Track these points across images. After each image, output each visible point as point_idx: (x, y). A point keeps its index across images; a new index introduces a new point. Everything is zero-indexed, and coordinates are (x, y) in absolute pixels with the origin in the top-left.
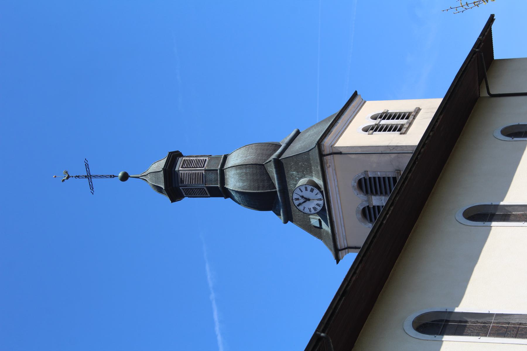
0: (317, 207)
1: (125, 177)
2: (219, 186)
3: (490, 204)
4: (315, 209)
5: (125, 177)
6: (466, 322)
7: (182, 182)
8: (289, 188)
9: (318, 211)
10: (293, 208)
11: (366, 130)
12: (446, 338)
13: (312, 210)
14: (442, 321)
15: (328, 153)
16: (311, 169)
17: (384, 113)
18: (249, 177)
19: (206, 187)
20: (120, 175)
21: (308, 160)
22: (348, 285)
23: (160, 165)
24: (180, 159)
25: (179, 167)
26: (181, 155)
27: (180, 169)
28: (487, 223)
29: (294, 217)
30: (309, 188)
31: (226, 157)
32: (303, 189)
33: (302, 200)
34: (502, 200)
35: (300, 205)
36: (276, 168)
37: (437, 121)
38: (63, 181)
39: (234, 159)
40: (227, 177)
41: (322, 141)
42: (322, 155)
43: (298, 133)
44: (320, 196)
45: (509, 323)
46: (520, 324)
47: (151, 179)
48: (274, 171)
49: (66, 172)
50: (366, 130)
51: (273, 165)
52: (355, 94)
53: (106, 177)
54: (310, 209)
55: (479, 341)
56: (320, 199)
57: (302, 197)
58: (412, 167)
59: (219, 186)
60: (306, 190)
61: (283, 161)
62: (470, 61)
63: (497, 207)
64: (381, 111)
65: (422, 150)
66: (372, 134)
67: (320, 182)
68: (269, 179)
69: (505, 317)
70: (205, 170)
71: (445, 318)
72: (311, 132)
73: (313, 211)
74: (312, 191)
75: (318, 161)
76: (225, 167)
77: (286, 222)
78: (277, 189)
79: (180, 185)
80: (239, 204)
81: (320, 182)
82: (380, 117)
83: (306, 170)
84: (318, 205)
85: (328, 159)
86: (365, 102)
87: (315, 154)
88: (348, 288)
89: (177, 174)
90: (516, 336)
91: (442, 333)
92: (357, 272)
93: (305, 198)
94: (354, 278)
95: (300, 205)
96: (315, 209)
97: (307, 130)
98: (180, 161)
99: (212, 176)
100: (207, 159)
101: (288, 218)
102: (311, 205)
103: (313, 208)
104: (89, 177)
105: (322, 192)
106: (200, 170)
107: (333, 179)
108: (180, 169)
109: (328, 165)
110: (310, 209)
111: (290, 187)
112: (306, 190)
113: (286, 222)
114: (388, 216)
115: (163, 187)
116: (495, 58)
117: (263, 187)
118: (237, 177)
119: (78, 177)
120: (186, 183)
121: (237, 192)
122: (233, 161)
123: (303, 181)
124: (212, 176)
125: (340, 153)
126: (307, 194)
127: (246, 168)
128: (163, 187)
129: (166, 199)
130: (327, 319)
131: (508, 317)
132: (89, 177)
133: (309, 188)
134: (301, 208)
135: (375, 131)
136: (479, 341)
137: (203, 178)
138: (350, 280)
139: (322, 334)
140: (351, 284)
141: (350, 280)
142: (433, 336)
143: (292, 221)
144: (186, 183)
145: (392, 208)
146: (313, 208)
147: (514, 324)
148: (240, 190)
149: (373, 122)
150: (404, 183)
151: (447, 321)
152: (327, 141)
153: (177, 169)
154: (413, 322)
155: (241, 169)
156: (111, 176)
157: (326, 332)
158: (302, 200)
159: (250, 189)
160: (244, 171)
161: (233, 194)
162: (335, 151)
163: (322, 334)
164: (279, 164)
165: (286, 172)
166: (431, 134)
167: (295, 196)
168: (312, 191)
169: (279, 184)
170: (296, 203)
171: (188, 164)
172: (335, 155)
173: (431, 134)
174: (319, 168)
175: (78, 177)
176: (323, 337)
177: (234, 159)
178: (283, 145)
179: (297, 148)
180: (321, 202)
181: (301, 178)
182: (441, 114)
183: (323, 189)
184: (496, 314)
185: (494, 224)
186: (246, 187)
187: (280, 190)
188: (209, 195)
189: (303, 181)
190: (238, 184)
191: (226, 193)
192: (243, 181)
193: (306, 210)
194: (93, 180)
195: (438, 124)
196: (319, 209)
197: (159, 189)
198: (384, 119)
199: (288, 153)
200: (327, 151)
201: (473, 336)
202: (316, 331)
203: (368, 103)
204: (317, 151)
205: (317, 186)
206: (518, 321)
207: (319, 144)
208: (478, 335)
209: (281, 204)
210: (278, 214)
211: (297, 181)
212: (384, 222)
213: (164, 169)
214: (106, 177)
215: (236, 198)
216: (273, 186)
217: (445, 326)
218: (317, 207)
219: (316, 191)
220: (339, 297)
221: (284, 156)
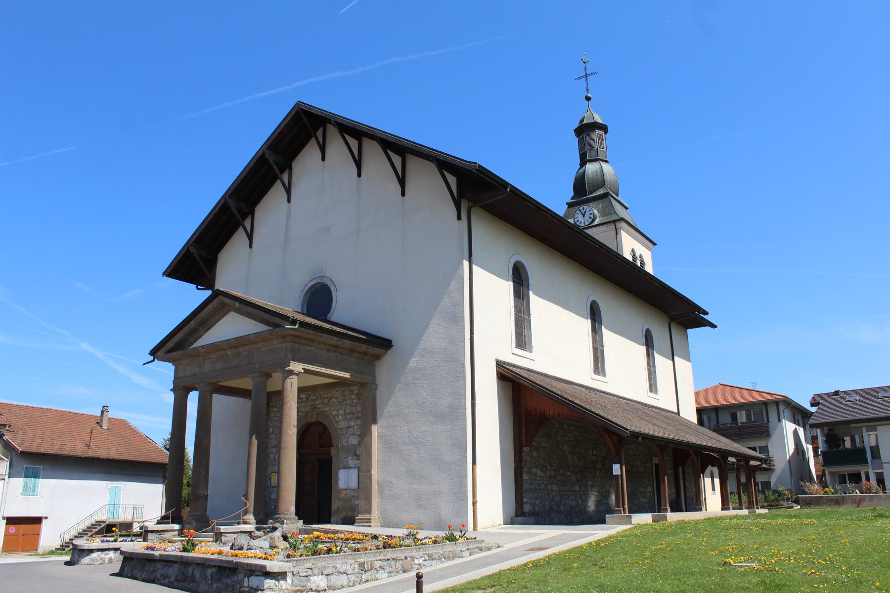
0: (580, 222)
1: (588, 99)
2: (588, 158)
3: (602, 319)
4: (578, 221)
5: (588, 99)
6: (523, 300)
7: (588, 135)
8: (590, 204)
9: (577, 223)
10: (577, 208)
11: (633, 251)
12: (511, 284)
13: (577, 219)
14: (522, 282)
15: (617, 226)
16: (604, 216)
17: (644, 263)
18: (596, 177)
19: (586, 151)
20: (589, 95)
21: (610, 214)
22: (544, 211)
23: (598, 119)
24: (603, 132)
25: (597, 132)
26: (606, 133)
27: (597, 133)
28: (589, 316)
29: (571, 209)
30: (592, 216)
31: (607, 162)
32: (591, 212)
33: (583, 212)
34: (605, 328)
35: (580, 210)
36: (603, 194)
37: (655, 282)
38: (582, 60)
39: (606, 168)
40: (594, 163)
41: (625, 222)
42: (614, 222)
43: (627, 208)
44: (587, 223)
45: (524, 329)
46: (525, 336)
47: (588, 115)
48: (601, 193)
49: (588, 61)
50: (633, 251)
51: (605, 192)
52: (654, 244)
53: (587, 86)
54: (577, 218)
55: (511, 307)
56: (585, 224)
57: (585, 212)
58: (625, 262)
59: (588, 158)
60: (590, 214)
61: (608, 198)
62: (694, 307)
63: (600, 323)
64: (645, 260)
65: (636, 270)
66: (631, 255)
67: (596, 223)
68: (595, 191)
69: (528, 326)
70: (597, 149)
71: (524, 283)
72: (627, 215)
73: (576, 220)
74: (590, 218)
75: (610, 220)
76: (600, 162)
77: (567, 204)
78: (589, 196)
79: (586, 134)
80: (577, 173)
81: (596, 223)
82: (641, 260)
83: (603, 213)
84: (581, 222)
85: (612, 226)
86: (650, 251)
87: (615, 218)
88: (542, 212)
89: (593, 131)
90: (516, 333)
91: (514, 281)
92: (554, 219)
93: (584, 214)
94: (549, 216)
95: (580, 210)
96: (578, 221)
97: (628, 213)
98: (602, 133)
99: (594, 153)
100: (605, 150)
101: (570, 205)
102: (580, 218)
103: (578, 220)
104: (586, 76)
105: (589, 224)
106: (597, 146)
107: (599, 230)
108: (597, 133)
109: (608, 227)
110: (577, 218)
111: (591, 204)
112: (590, 214)
113: (567, 204)
114: (592, 243)
115: (584, 123)
116: (688, 330)
117: (589, 187)
118: (595, 169)
119: (586, 69)
120: (588, 137)
121: (585, 170)
122: (604, 165)
123: (596, 212)
124: (594, 153)
125: (617, 234)
126: (587, 215)
127: (601, 175)
128: (584, 123)
129: (576, 125)
130: (519, 194)
131: (529, 328)
132: (586, 76)
133: (592, 216)
134: (578, 212)
135: (633, 257)
136: (511, 307)
137: (592, 148)
138: (548, 213)
139: (509, 189)
140: (544, 213)
141: (548, 213)
142: (511, 275)
143: (568, 208)
144: (588, 137)
145: (597, 246)
146: (578, 220)
147: (524, 332)
148: (586, 172)
149: (638, 255)
150: (615, 256)
151: (522, 286)
152: (624, 225)
153: (596, 130)
154: (520, 261)
155: (600, 171)
156: (588, 90)
157: (510, 193)
158: (583, 212)
159: (587, 179)
160: (599, 174)
161: (583, 168)
162: (618, 230)
163: (509, 189)
164: (606, 195)
165: (601, 200)
166: (647, 277)
167: (585, 207)
168: (590, 218)
169: (592, 197)
170: (581, 208)
171: (601, 138)
172: (615, 231)
173: (647, 277)
174: (606, 221)
175: (586, 69)
176: (507, 189)
177: (606, 168)
178: (618, 198)
179: (618, 207)
180: (583, 225)
181: (598, 211)
182: (660, 285)
183: (591, 225)
184: (530, 320)
185: (589, 321)
186: (588, 176)
187: (588, 198)
188: (581, 153)
189: (596, 212)
190: (590, 170)
191: (583, 163)
192: (592, 174)
193: (576, 216)
194: (584, 79)
195: (653, 282)
196: (578, 224)
197: (582, 120)
198: (641, 263)
199: (613, 200)
200: (618, 225)
201: (514, 303)
202: (511, 185)
203: (650, 252)
204: (617, 219)
205: (592, 222)
206: (526, 334)
207: (622, 219)
208: (515, 307)
209: (579, 199)
210: (572, 199)
211: (595, 208)
212: (588, 241)
213: (595, 122)
214: (587, 86)
215: (581, 171)
216: (591, 193)
217: (519, 283)
218: (580, 222)
219: (590, 220)
220: (535, 203)
221: (611, 198)
